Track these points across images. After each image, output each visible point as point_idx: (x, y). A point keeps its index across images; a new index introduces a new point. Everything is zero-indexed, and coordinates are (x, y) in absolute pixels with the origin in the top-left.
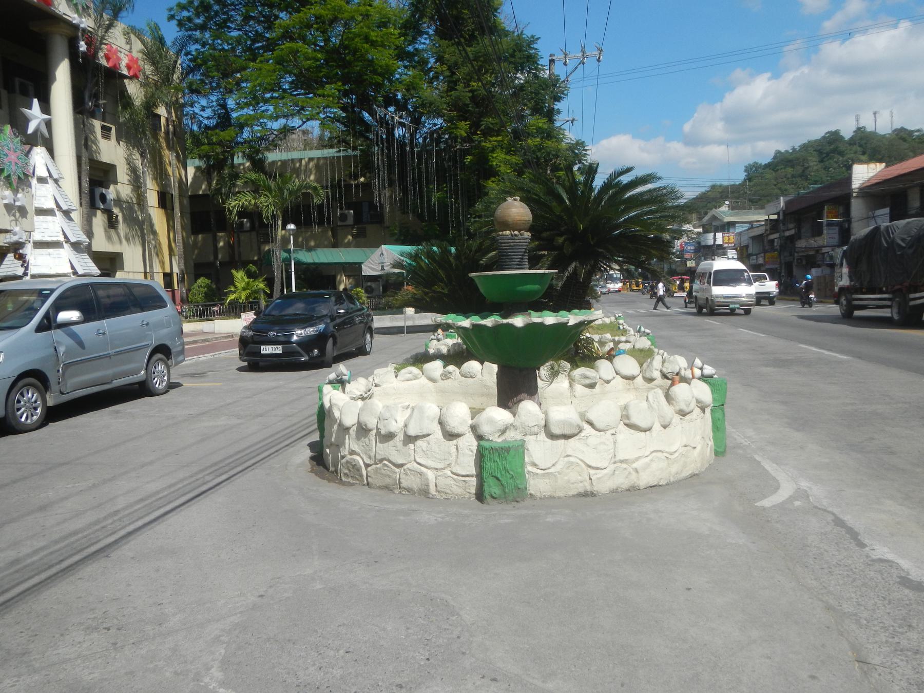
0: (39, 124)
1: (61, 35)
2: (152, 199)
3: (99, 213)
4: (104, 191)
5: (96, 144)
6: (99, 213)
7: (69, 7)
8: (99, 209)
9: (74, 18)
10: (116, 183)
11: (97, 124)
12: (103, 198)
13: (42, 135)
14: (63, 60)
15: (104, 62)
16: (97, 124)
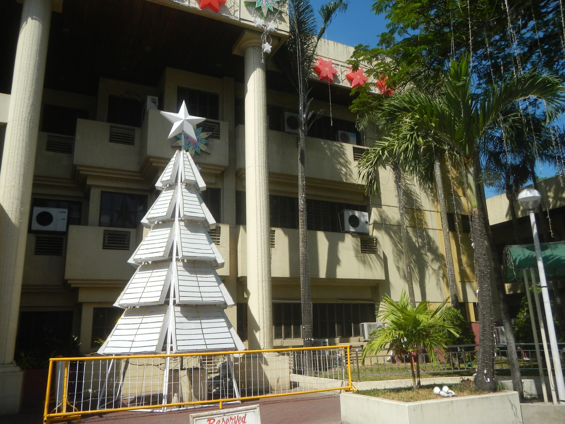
0: (182, 124)
1: (253, 47)
2: (434, 220)
3: (349, 238)
4: (357, 213)
5: (346, 167)
6: (349, 238)
7: (250, 13)
8: (348, 232)
9: (257, 21)
10: (379, 205)
11: (349, 148)
12: (355, 221)
13: (187, 137)
14: (254, 70)
15: (346, 84)
16: (349, 148)
